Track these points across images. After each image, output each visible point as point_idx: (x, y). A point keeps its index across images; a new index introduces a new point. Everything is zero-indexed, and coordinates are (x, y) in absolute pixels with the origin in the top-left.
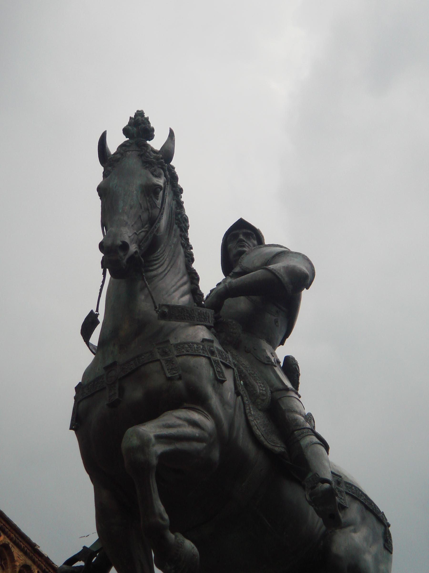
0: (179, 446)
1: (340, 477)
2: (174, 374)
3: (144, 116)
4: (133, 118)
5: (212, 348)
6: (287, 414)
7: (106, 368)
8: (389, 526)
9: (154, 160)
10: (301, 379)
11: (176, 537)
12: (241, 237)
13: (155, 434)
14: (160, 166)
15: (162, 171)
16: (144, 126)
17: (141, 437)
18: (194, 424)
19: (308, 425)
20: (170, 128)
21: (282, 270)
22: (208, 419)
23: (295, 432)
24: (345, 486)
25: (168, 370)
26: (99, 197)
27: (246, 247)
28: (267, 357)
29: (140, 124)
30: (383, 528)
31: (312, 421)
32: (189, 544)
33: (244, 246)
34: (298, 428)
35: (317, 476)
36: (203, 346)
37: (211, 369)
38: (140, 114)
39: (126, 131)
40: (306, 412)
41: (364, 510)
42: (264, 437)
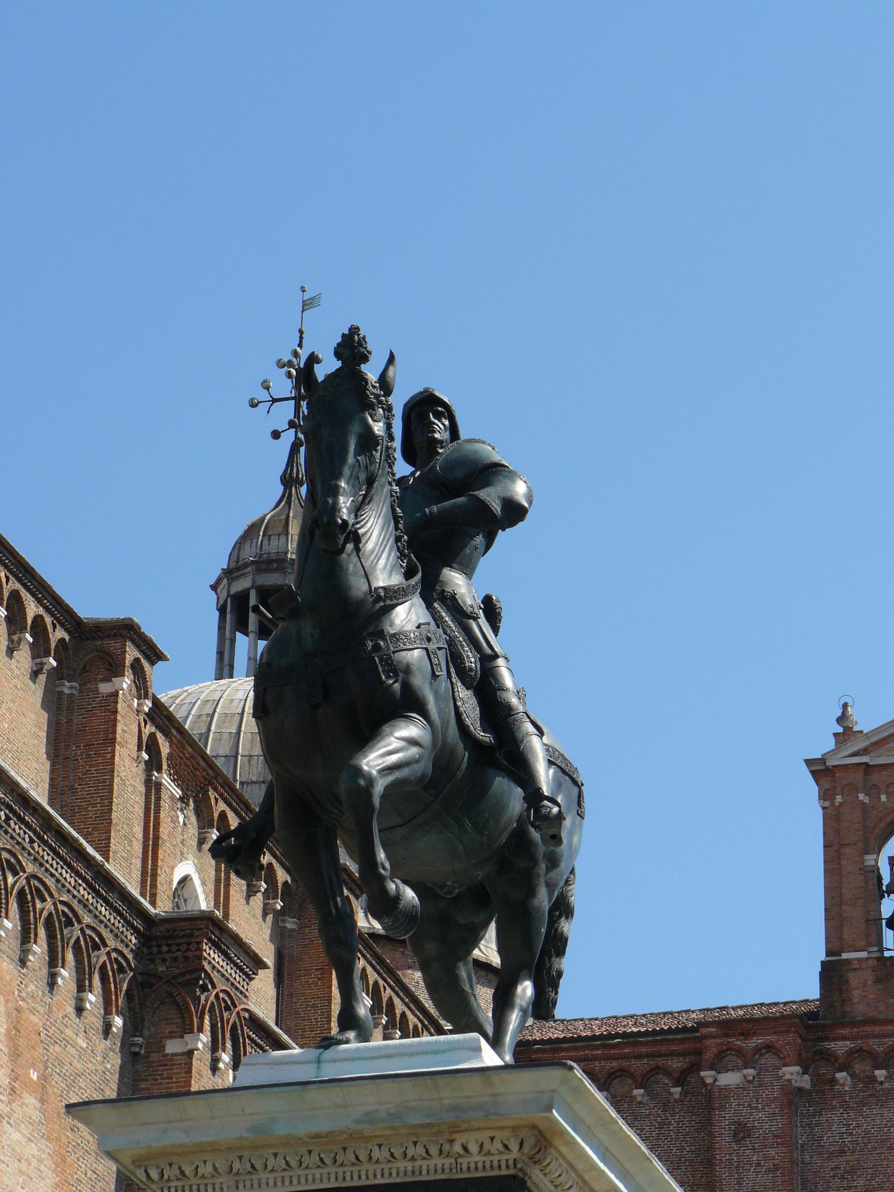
4: (346, 334)
6: (498, 693)
8: (582, 785)
11: (397, 887)
18: (412, 742)
20: (391, 351)
32: (409, 894)
38: (354, 330)
39: (338, 354)
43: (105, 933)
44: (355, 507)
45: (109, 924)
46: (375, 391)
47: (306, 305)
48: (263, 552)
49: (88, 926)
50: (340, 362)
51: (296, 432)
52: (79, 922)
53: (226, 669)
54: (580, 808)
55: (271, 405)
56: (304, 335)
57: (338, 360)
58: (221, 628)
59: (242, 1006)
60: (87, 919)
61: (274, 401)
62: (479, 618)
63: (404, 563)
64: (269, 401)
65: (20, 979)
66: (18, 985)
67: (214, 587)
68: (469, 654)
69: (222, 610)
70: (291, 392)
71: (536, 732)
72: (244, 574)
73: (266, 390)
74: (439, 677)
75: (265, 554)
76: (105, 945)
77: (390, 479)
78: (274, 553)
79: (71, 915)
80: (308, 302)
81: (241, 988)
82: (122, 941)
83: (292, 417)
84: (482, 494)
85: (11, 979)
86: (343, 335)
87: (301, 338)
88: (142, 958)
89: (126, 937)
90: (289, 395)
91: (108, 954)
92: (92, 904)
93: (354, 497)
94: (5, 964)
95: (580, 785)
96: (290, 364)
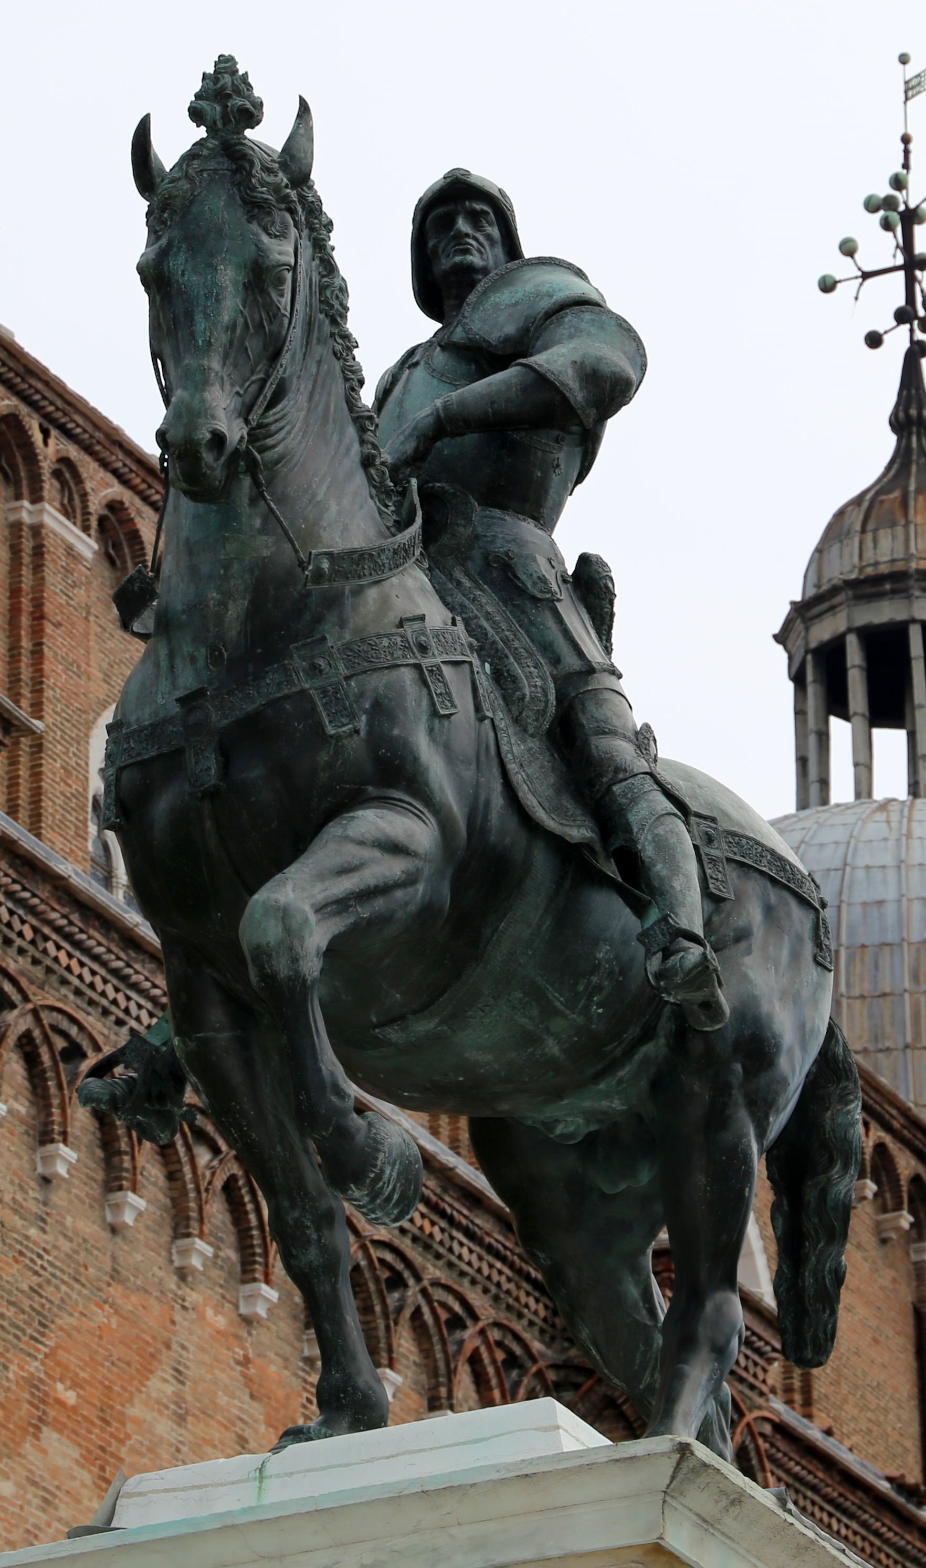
0: (365, 912)
1: (713, 820)
2: (344, 725)
3: (237, 71)
5: (423, 638)
7: (182, 701)
9: (270, 197)
10: (619, 606)
12: (462, 225)
13: (313, 901)
14: (283, 206)
15: (288, 216)
16: (240, 103)
17: (284, 914)
18: (394, 848)
19: (642, 765)
20: (300, 97)
21: (570, 372)
22: (423, 821)
23: (615, 788)
24: (726, 842)
25: (328, 715)
26: (143, 288)
27: (475, 252)
28: (539, 578)
29: (229, 96)
30: (812, 916)
31: (652, 743)
33: (466, 252)
34: (621, 776)
35: (671, 921)
36: (402, 637)
37: (425, 691)
38: (226, 64)
39: (196, 115)
40: (638, 719)
41: (769, 885)
42: (544, 809)
43: (476, 1298)
44: (243, 404)
45: (479, 1278)
46: (270, 179)
47: (910, 89)
48: (864, 563)
49: (436, 1283)
50: (203, 128)
51: (912, 331)
52: (418, 1278)
53: (814, 789)
54: (821, 949)
55: (861, 284)
56: (912, 146)
57: (198, 126)
58: (800, 712)
59: (757, 1413)
60: (433, 1271)
61: (866, 276)
62: (559, 600)
63: (387, 506)
64: (857, 278)
65: (305, 1395)
66: (304, 1407)
67: (780, 638)
68: (532, 669)
69: (798, 678)
70: (894, 256)
71: (670, 807)
72: (832, 608)
73: (849, 259)
74: (453, 717)
75: (869, 565)
76: (475, 1318)
77: (339, 348)
78: (885, 562)
79: (400, 1266)
80: (913, 83)
81: (751, 1380)
82: (509, 1308)
83: (901, 301)
84: (540, 360)
85: (288, 1396)
86: (205, 76)
87: (907, 152)
88: (553, 1339)
89: (517, 1299)
90: (890, 264)
91: (482, 1332)
92: (441, 1243)
93: (241, 386)
94: (273, 1368)
95: (817, 906)
96: (889, 203)
